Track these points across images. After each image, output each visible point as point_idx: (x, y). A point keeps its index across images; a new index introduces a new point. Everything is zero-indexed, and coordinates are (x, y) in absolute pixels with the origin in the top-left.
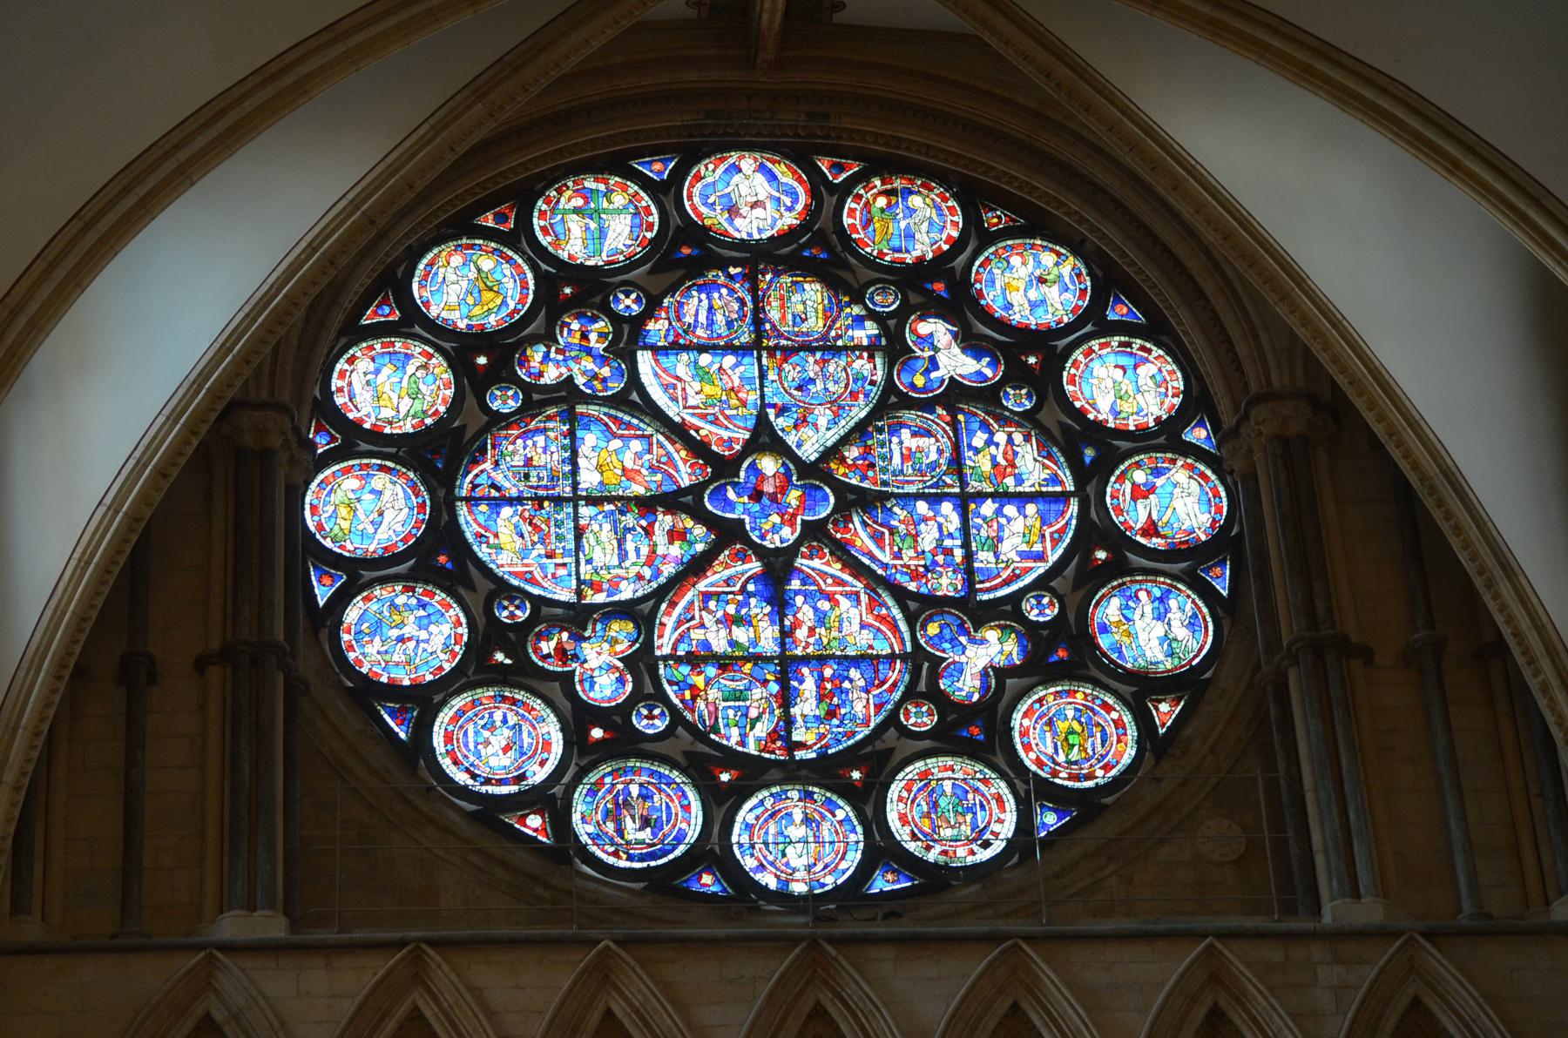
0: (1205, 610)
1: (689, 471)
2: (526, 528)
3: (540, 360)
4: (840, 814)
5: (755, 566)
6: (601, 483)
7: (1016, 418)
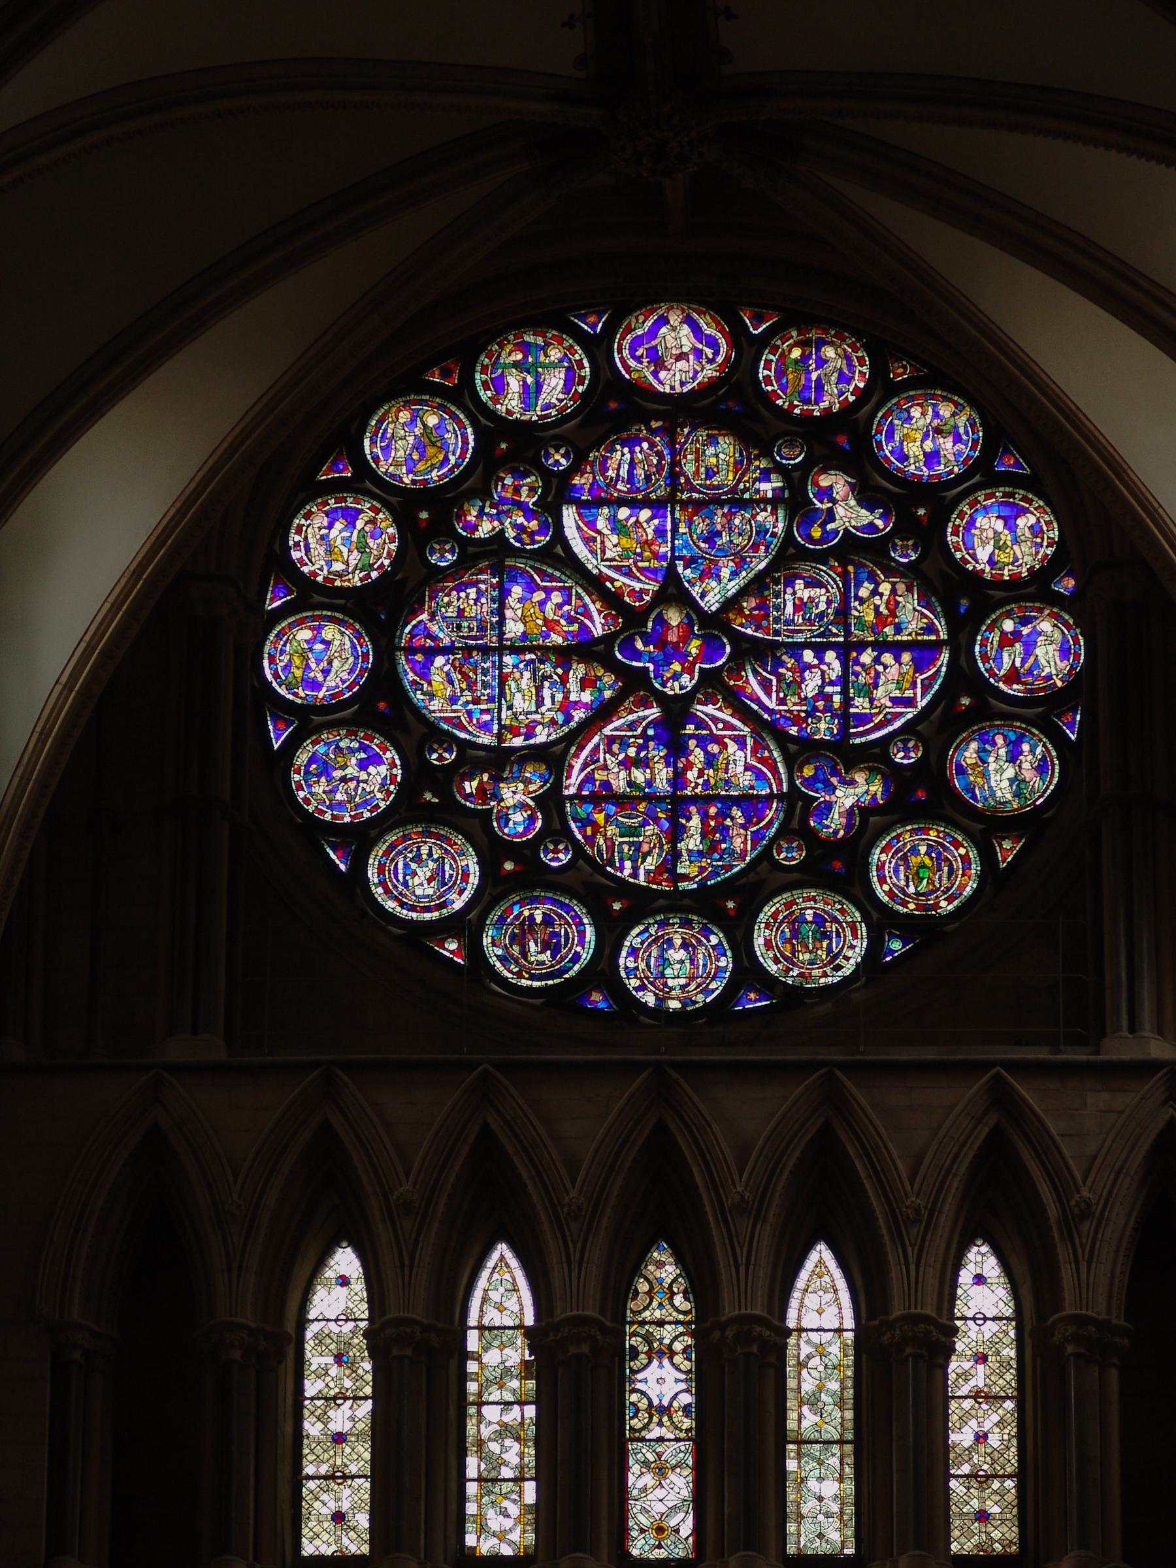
0: (1054, 754)
1: (603, 621)
2: (456, 676)
3: (475, 514)
4: (714, 940)
5: (654, 712)
6: (524, 634)
7: (901, 569)
